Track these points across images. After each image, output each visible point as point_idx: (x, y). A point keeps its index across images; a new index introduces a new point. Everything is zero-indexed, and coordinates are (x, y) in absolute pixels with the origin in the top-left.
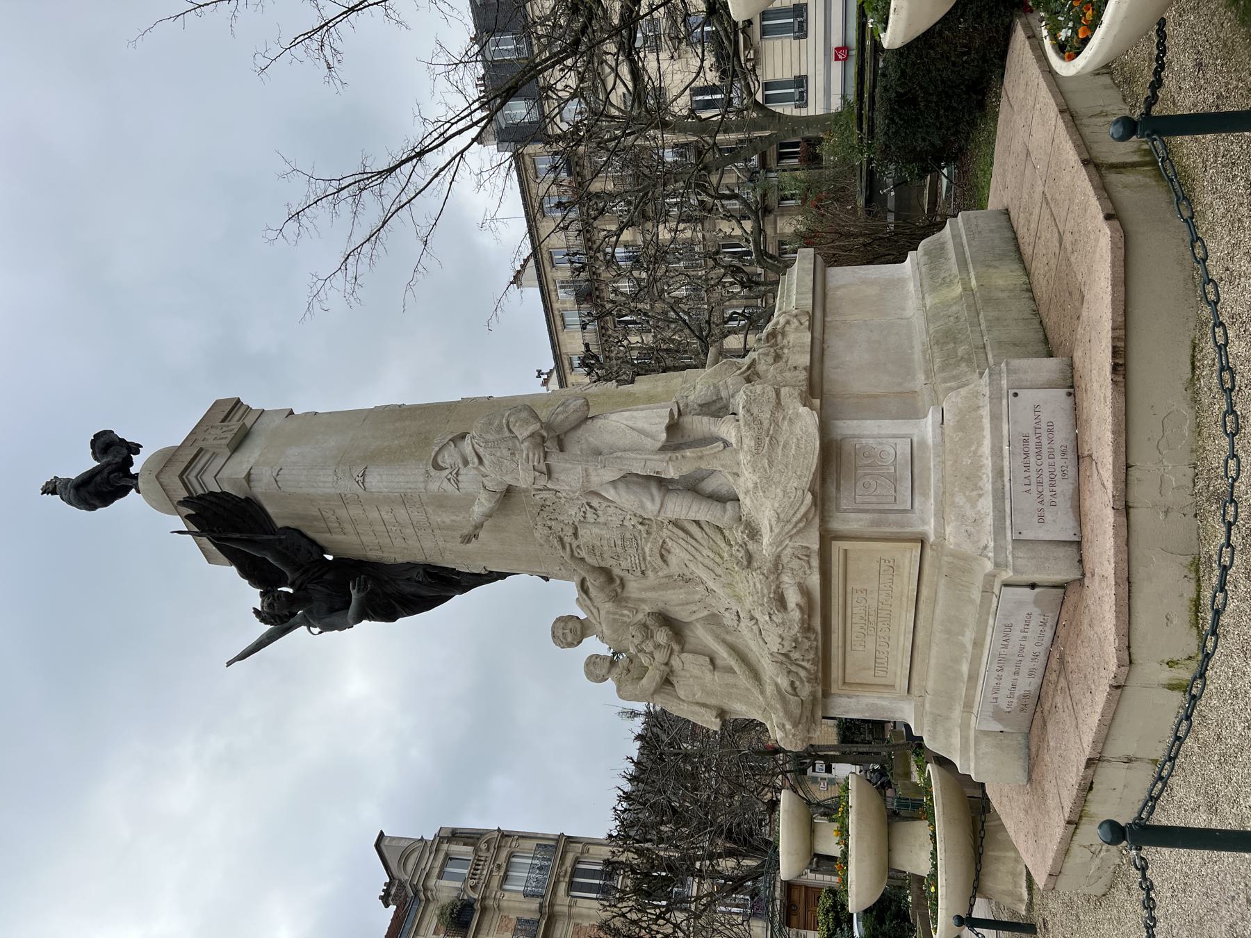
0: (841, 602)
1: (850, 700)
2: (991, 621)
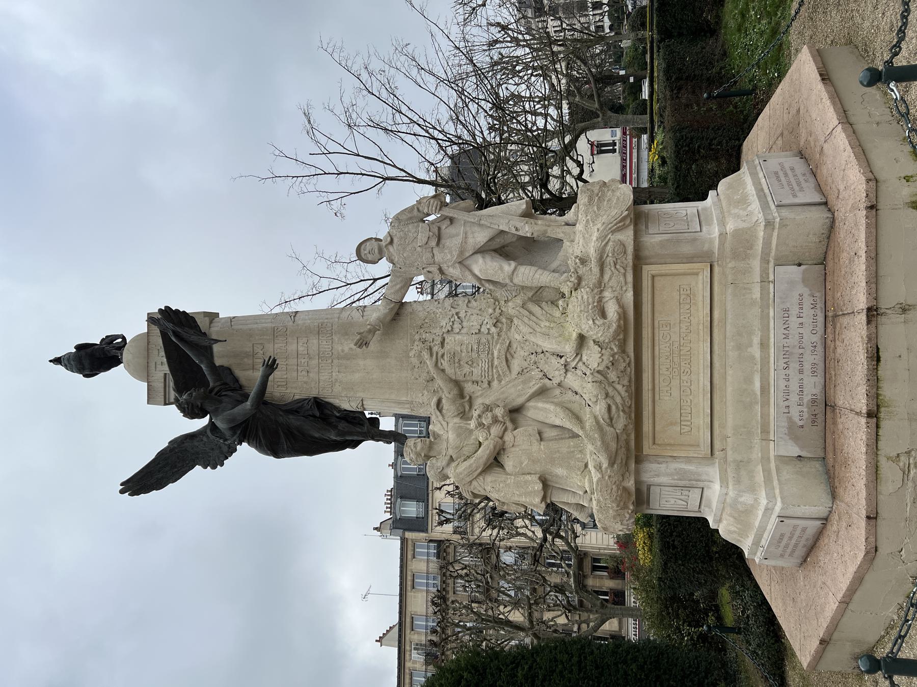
0: (650, 335)
1: (661, 465)
2: (771, 314)
